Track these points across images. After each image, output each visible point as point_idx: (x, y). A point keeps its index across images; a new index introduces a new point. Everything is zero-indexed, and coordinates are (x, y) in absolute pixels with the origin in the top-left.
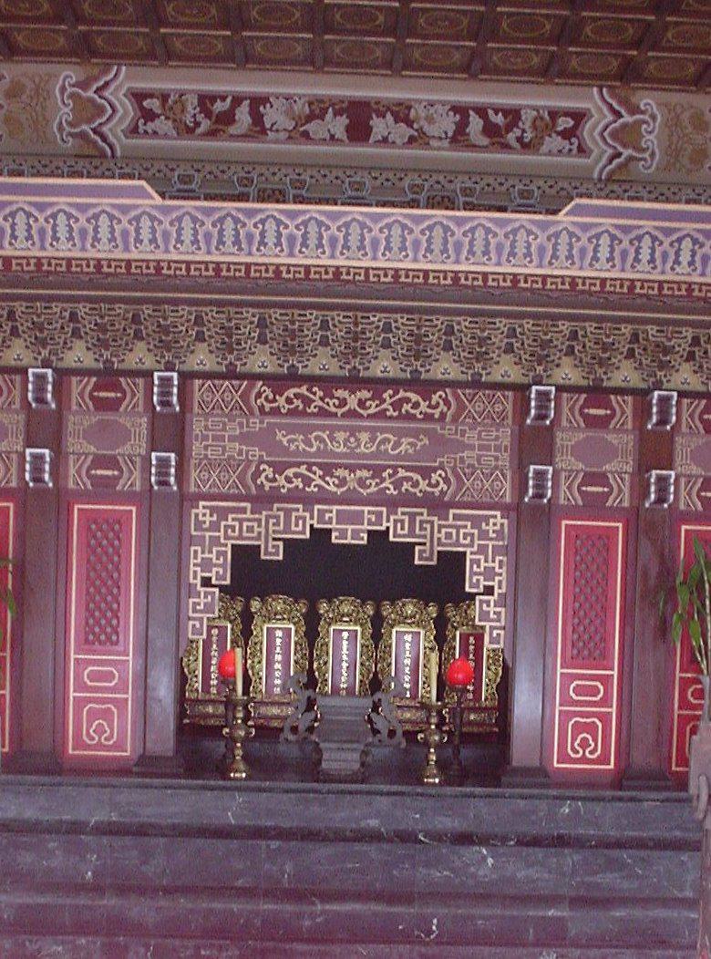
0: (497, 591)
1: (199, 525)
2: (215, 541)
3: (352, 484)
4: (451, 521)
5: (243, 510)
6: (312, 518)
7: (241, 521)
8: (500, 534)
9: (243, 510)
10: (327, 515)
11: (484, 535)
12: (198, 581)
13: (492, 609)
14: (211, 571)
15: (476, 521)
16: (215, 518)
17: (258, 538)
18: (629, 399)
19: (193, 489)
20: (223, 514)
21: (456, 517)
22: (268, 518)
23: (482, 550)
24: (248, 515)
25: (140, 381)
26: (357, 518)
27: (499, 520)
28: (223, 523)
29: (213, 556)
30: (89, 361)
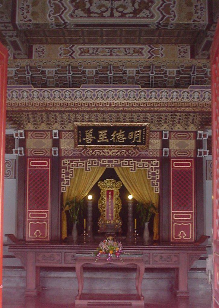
0: (156, 179)
1: (64, 164)
2: (69, 168)
3: (110, 153)
4: (141, 162)
5: (78, 161)
6: (101, 162)
7: (78, 163)
8: (157, 165)
9: (78, 161)
10: (104, 161)
11: (152, 165)
12: (64, 178)
13: (155, 183)
14: (69, 175)
15: (149, 162)
16: (69, 162)
17: (83, 166)
18: (192, 133)
19: (63, 155)
20: (72, 161)
21: (143, 161)
22: (86, 162)
23: (152, 168)
24: (80, 162)
25: (49, 132)
26: (112, 162)
27: (156, 162)
28: (71, 163)
29: (70, 171)
30: (32, 128)
